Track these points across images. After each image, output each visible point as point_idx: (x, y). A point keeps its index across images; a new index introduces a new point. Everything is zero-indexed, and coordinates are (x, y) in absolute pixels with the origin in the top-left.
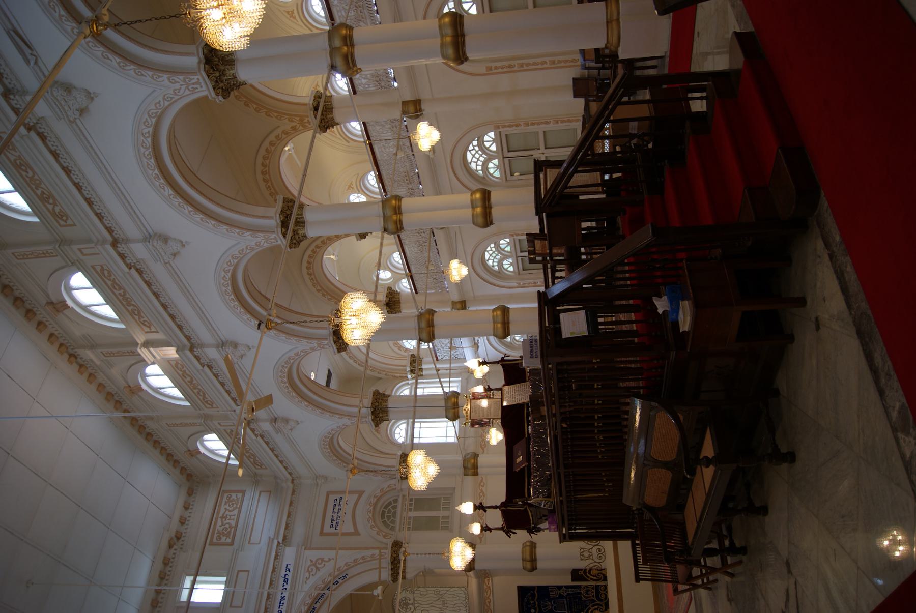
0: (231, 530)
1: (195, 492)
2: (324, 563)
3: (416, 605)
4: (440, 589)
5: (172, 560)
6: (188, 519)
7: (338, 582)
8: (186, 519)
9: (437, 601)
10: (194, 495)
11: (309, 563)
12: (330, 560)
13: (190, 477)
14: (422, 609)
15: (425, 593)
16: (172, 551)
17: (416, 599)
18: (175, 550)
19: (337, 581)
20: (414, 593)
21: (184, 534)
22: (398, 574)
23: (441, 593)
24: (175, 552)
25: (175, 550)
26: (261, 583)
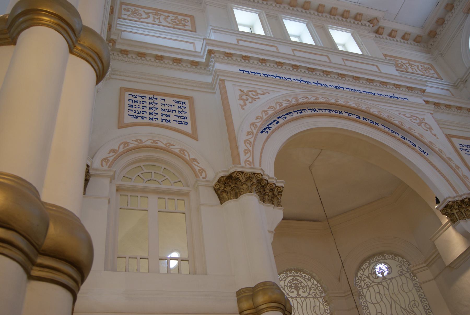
0: (402, 68)
1: (419, 44)
2: (429, 130)
3: (384, 284)
4: (421, 308)
5: (360, 23)
6: (395, 39)
7: (415, 146)
8: (395, 38)
9: (401, 307)
10: (416, 44)
11: (420, 117)
12: (435, 135)
13: (433, 34)
14: (382, 292)
15: (407, 290)
16: (368, 24)
17: (394, 281)
18: (369, 26)
19: (415, 145)
20: (400, 275)
21: (381, 36)
22: (442, 229)
23: (415, 310)
24: (367, 25)
25: (369, 26)
26: (385, 64)
